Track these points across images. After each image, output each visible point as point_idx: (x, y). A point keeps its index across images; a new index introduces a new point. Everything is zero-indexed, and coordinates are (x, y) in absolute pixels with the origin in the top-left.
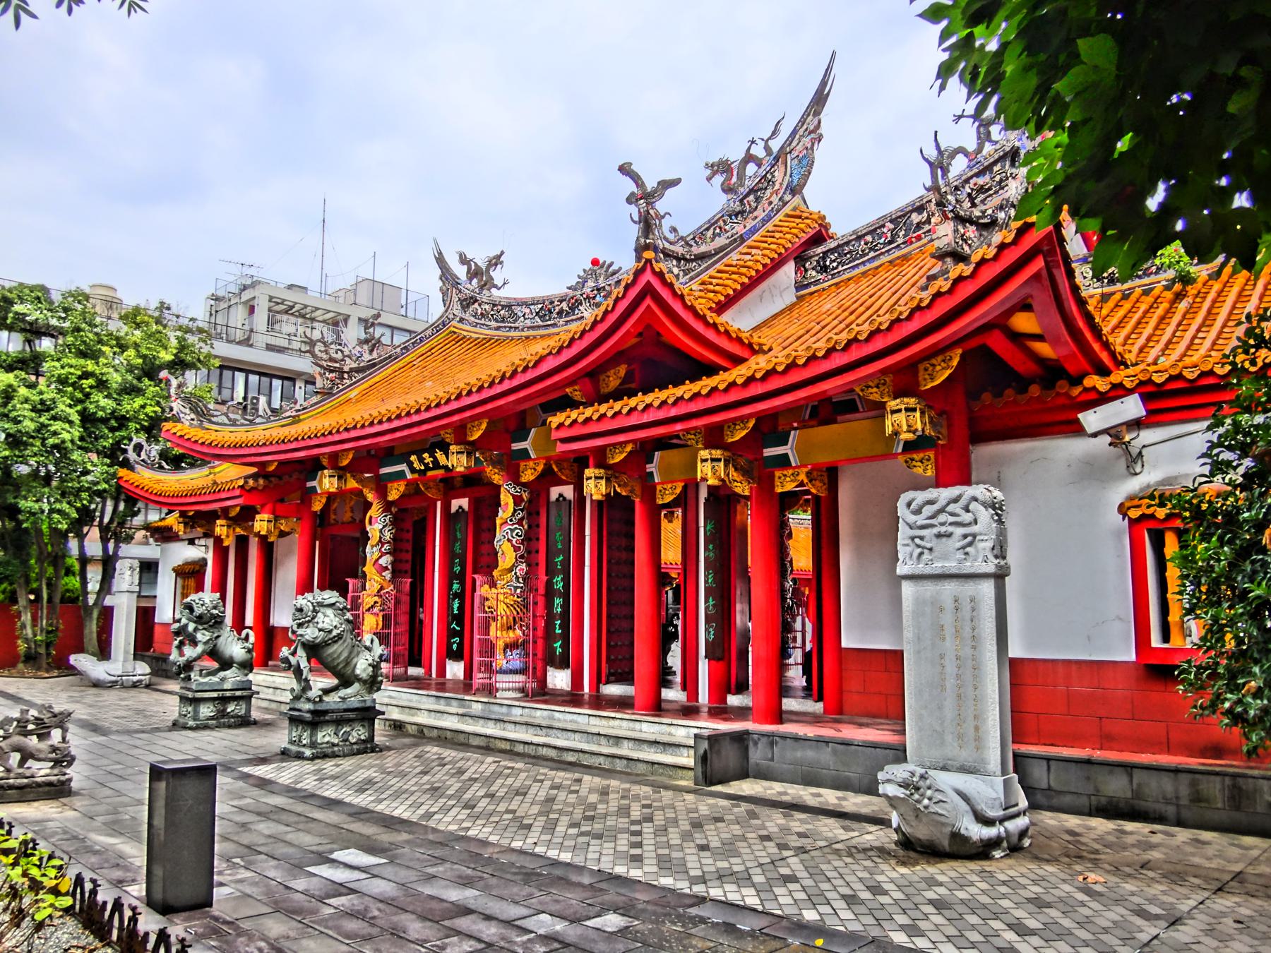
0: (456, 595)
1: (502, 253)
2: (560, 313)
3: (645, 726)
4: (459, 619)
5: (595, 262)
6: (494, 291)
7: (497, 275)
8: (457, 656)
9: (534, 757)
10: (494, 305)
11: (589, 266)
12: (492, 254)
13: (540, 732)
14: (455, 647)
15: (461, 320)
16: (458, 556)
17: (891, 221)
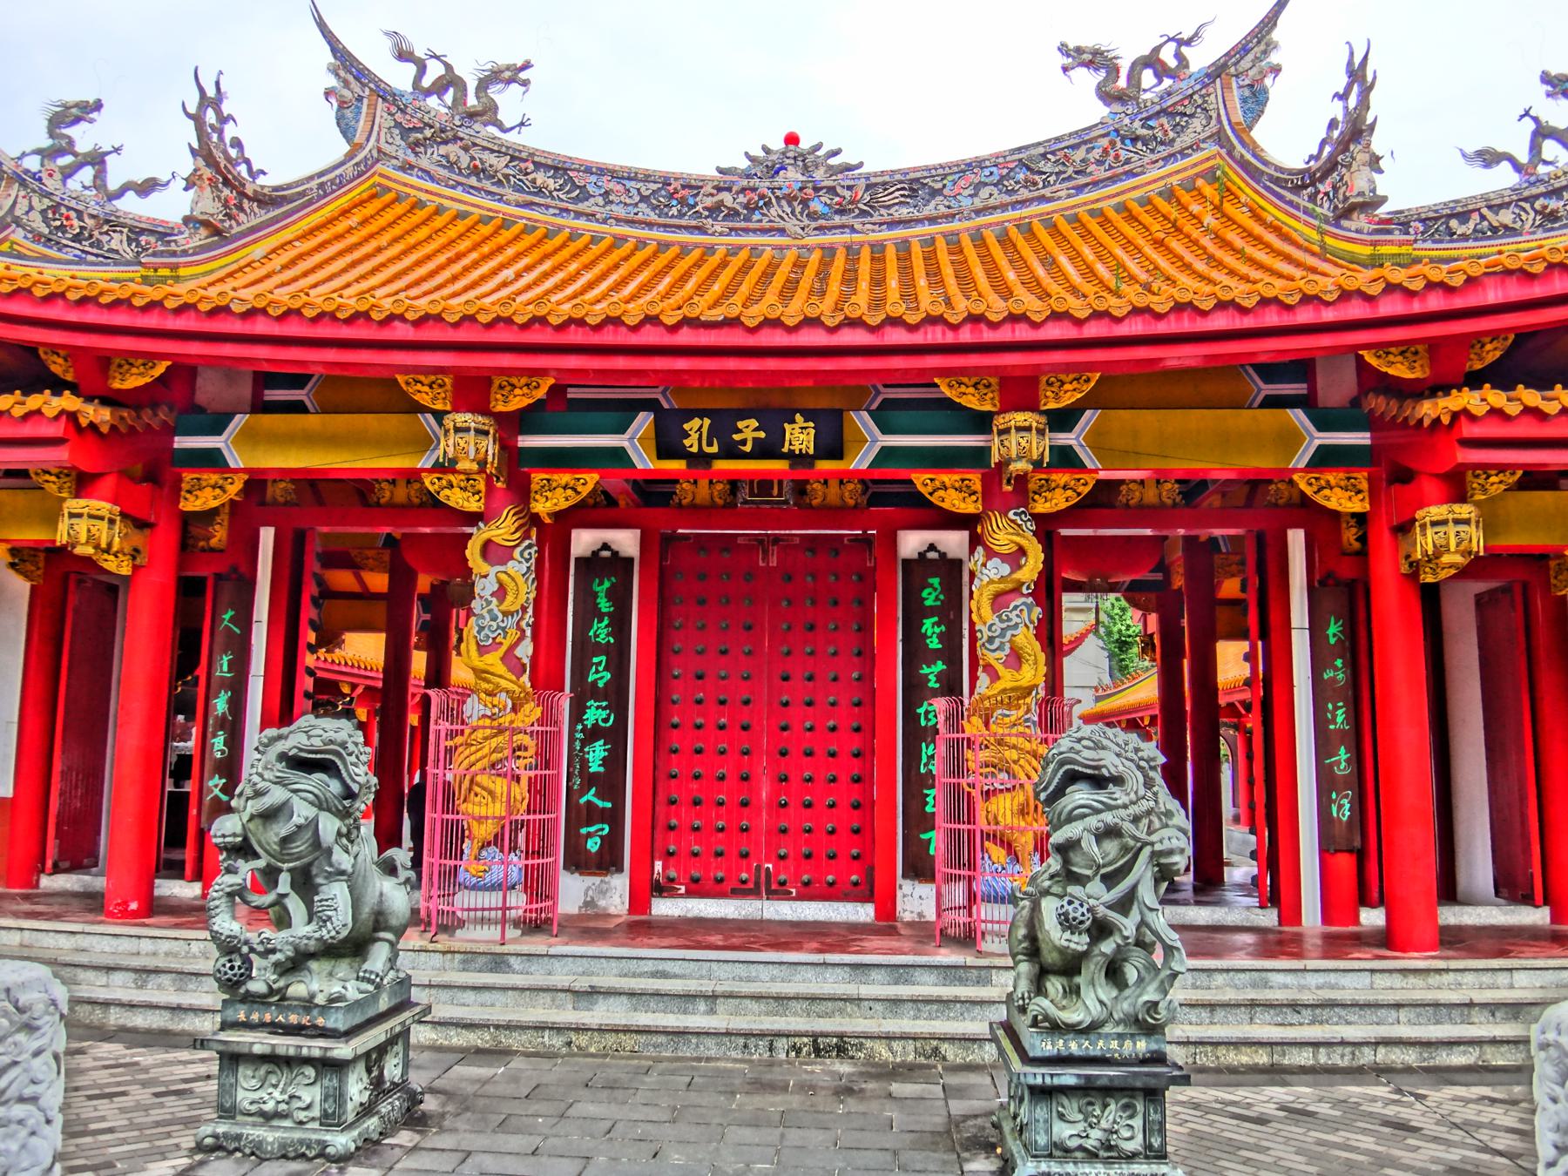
0: (593, 734)
1: (527, 66)
2: (713, 211)
3: (1521, 978)
4: (610, 782)
5: (792, 139)
6: (492, 130)
7: (509, 102)
8: (607, 862)
9: (1218, 1070)
10: (513, 158)
11: (778, 144)
12: (504, 60)
13: (1295, 1018)
14: (593, 845)
15: (407, 167)
16: (599, 649)
17: (1423, 221)
